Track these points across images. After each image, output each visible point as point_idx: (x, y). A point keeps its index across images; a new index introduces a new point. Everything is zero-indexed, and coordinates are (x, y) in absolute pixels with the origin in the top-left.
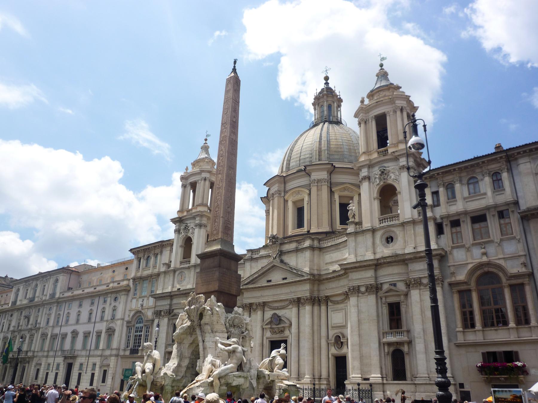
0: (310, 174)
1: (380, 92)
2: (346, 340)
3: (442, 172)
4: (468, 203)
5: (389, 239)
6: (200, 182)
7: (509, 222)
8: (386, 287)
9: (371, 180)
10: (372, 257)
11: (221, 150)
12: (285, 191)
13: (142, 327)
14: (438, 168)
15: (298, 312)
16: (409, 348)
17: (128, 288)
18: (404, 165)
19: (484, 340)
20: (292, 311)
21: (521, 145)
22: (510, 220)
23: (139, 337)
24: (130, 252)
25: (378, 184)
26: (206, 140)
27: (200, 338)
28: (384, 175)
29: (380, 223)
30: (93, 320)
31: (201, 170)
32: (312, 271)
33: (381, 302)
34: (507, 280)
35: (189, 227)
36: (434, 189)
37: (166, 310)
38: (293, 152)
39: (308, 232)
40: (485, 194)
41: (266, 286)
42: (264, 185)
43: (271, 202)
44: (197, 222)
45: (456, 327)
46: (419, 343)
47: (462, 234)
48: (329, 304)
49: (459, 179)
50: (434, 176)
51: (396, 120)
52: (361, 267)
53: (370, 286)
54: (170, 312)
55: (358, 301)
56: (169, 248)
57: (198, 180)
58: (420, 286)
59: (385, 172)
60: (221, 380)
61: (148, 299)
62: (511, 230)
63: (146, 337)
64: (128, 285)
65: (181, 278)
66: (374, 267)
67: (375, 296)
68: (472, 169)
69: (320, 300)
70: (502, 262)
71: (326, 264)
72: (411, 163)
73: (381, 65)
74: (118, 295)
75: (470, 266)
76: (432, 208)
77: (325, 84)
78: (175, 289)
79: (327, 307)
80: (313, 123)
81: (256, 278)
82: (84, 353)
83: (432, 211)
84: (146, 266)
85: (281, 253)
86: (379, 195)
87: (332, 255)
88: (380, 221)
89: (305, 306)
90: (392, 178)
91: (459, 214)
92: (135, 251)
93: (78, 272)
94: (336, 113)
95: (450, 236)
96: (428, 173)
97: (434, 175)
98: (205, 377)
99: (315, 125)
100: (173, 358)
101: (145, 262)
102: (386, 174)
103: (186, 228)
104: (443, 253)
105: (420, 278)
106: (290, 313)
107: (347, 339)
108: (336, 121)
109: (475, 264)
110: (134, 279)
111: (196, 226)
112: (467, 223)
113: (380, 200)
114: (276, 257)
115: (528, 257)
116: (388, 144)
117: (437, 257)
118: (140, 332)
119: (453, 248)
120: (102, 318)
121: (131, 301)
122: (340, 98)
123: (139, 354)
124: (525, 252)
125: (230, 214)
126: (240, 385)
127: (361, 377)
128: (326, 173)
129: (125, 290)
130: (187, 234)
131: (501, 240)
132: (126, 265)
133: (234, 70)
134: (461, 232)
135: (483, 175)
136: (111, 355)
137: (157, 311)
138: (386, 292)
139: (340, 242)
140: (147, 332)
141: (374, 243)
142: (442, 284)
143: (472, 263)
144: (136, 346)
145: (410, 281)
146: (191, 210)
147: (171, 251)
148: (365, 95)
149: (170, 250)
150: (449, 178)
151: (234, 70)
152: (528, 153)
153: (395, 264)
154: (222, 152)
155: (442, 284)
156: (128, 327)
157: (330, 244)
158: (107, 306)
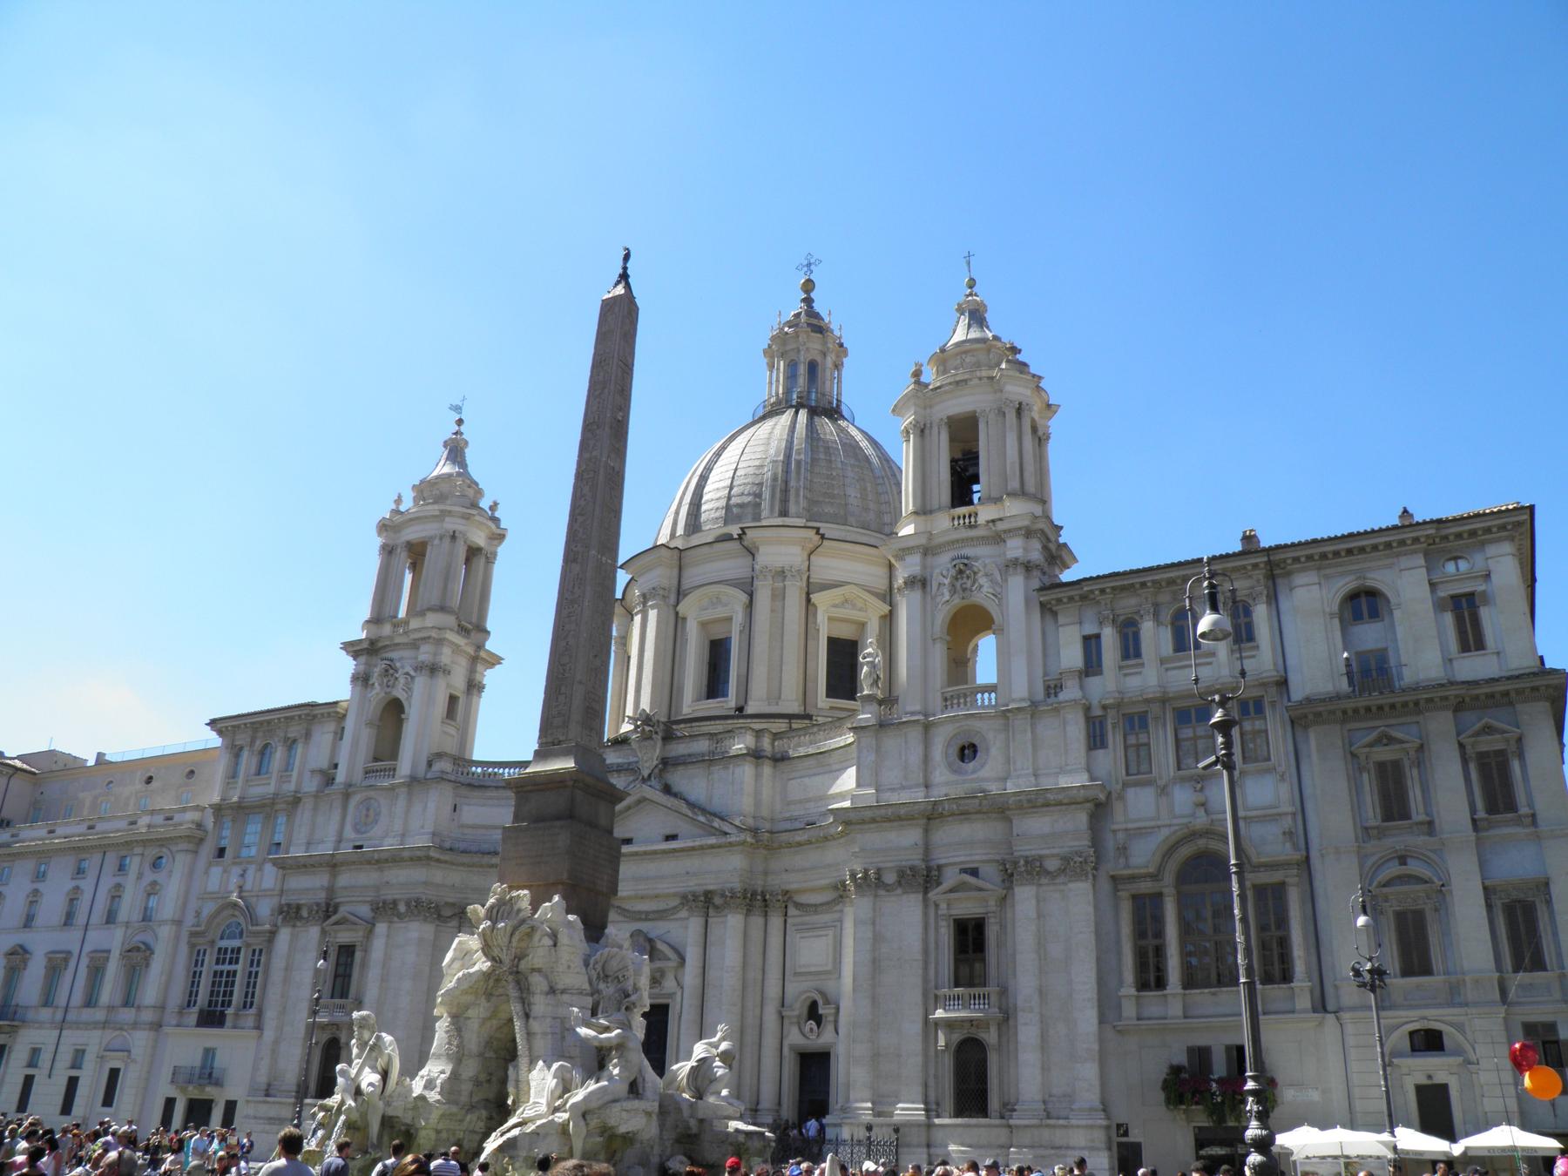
0: (753, 551)
1: (964, 356)
2: (833, 1011)
3: (1113, 588)
4: (1170, 673)
5: (966, 752)
6: (437, 542)
7: (1263, 728)
8: (951, 878)
9: (928, 589)
10: (918, 796)
11: (582, 496)
12: (679, 591)
13: (239, 949)
14: (1105, 577)
15: (703, 931)
16: (1000, 1036)
17: (199, 834)
18: (1017, 559)
19: (1185, 1017)
20: (686, 928)
21: (1303, 541)
22: (1266, 724)
23: (228, 976)
24: (209, 728)
26: (460, 422)
28: (965, 580)
29: (946, 707)
30: (80, 919)
31: (442, 511)
33: (936, 913)
35: (397, 671)
36: (1090, 629)
37: (318, 905)
38: (709, 482)
39: (740, 709)
43: (638, 619)
44: (422, 657)
45: (1121, 983)
46: (1026, 1024)
47: (1149, 749)
48: (792, 911)
49: (1152, 610)
50: (1092, 596)
53: (908, 872)
54: (327, 911)
55: (874, 910)
56: (331, 727)
57: (432, 538)
58: (1040, 878)
59: (968, 572)
60: (588, 1117)
61: (260, 869)
62: (1265, 748)
63: (250, 976)
64: (199, 825)
65: (367, 816)
66: (925, 821)
67: (920, 896)
69: (765, 900)
71: (789, 804)
72: (1036, 554)
73: (972, 283)
74: (164, 850)
75: (1165, 832)
76: (1080, 678)
77: (804, 300)
79: (785, 921)
80: (764, 407)
83: (1082, 687)
84: (258, 773)
86: (945, 631)
87: (806, 780)
88: (946, 700)
89: (726, 916)
90: (985, 589)
92: (227, 727)
94: (828, 383)
96: (1078, 586)
97: (1092, 592)
98: (543, 1109)
99: (772, 412)
100: (438, 1057)
101: (255, 760)
102: (968, 577)
103: (390, 671)
104: (1102, 797)
105: (1041, 858)
107: (838, 1009)
108: (827, 406)
109: (1177, 828)
110: (218, 809)
111: (419, 668)
112: (1165, 725)
113: (948, 642)
114: (650, 776)
115: (1299, 818)
116: (976, 497)
118: (230, 963)
119: (1125, 785)
120: (111, 918)
121: (207, 872)
122: (841, 345)
124: (1293, 805)
126: (634, 1134)
127: (872, 1109)
128: (796, 550)
129: (189, 838)
130: (388, 690)
132: (188, 766)
133: (624, 277)
134: (1148, 745)
136: (135, 1025)
137: (289, 905)
138: (951, 891)
139: (833, 747)
140: (252, 965)
141: (926, 759)
142: (1094, 876)
144: (217, 1002)
145: (1015, 863)
146: (406, 622)
147: (339, 734)
148: (925, 361)
149: (336, 733)
150: (1128, 604)
151: (624, 277)
152: (1318, 563)
153: (978, 816)
154: (582, 503)
155: (1094, 877)
156: (192, 946)
157: (802, 751)
158: (130, 882)
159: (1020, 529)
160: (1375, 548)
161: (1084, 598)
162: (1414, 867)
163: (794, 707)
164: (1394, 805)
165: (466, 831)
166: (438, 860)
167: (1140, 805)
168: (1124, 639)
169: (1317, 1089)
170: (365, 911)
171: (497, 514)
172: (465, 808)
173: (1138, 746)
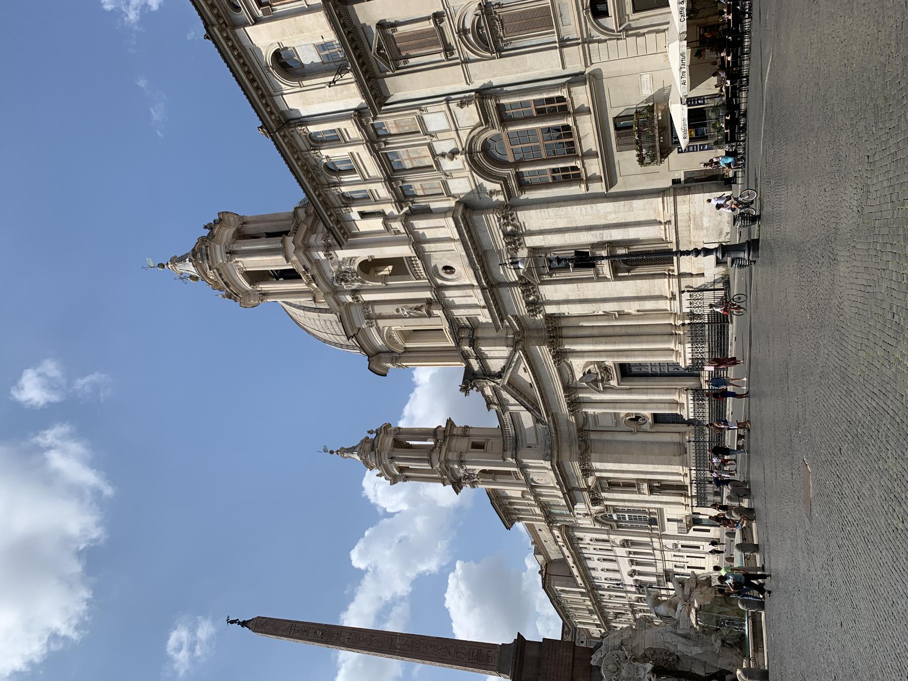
3: (327, 210)
10: (479, 291)
18: (325, 255)
25: (362, 282)
26: (332, 452)
32: (510, 342)
34: (493, 127)
37: (590, 495)
41: (540, 391)
44: (456, 466)
46: (611, 236)
52: (496, 305)
61: (577, 509)
66: (495, 290)
68: (312, 171)
78: (558, 487)
81: (528, 401)
82: (660, 565)
85: (487, 374)
93: (547, 564)
102: (344, 276)
104: (461, 209)
106: (578, 365)
119: (449, 195)
123: (656, 517)
125: (459, 650)
131: (426, 134)
153: (486, 266)
159: (306, 255)
160: (244, 65)
161: (338, 222)
162: (468, 25)
165: (540, 440)
166: (558, 457)
169: (641, 75)
170: (591, 480)
171: (374, 430)
172: (528, 442)
173: (423, 189)
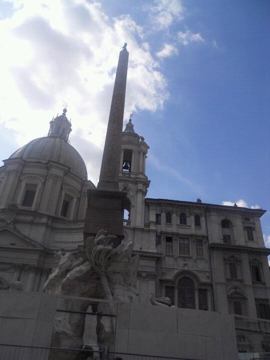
27: (107, 289)
40: (190, 226)
42: (3, 161)
51: (139, 159)
70: (195, 272)
75: (176, 271)
85: (16, 222)
89: (29, 274)
91: (173, 234)
95: (165, 247)
117: (157, 259)
119: (166, 255)
134: (172, 246)
135: (191, 214)
143: (177, 269)
150: (170, 209)
161: (158, 204)
162: (237, 290)
163: (54, 215)
164: (234, 274)
167: (168, 262)
168: (167, 217)
